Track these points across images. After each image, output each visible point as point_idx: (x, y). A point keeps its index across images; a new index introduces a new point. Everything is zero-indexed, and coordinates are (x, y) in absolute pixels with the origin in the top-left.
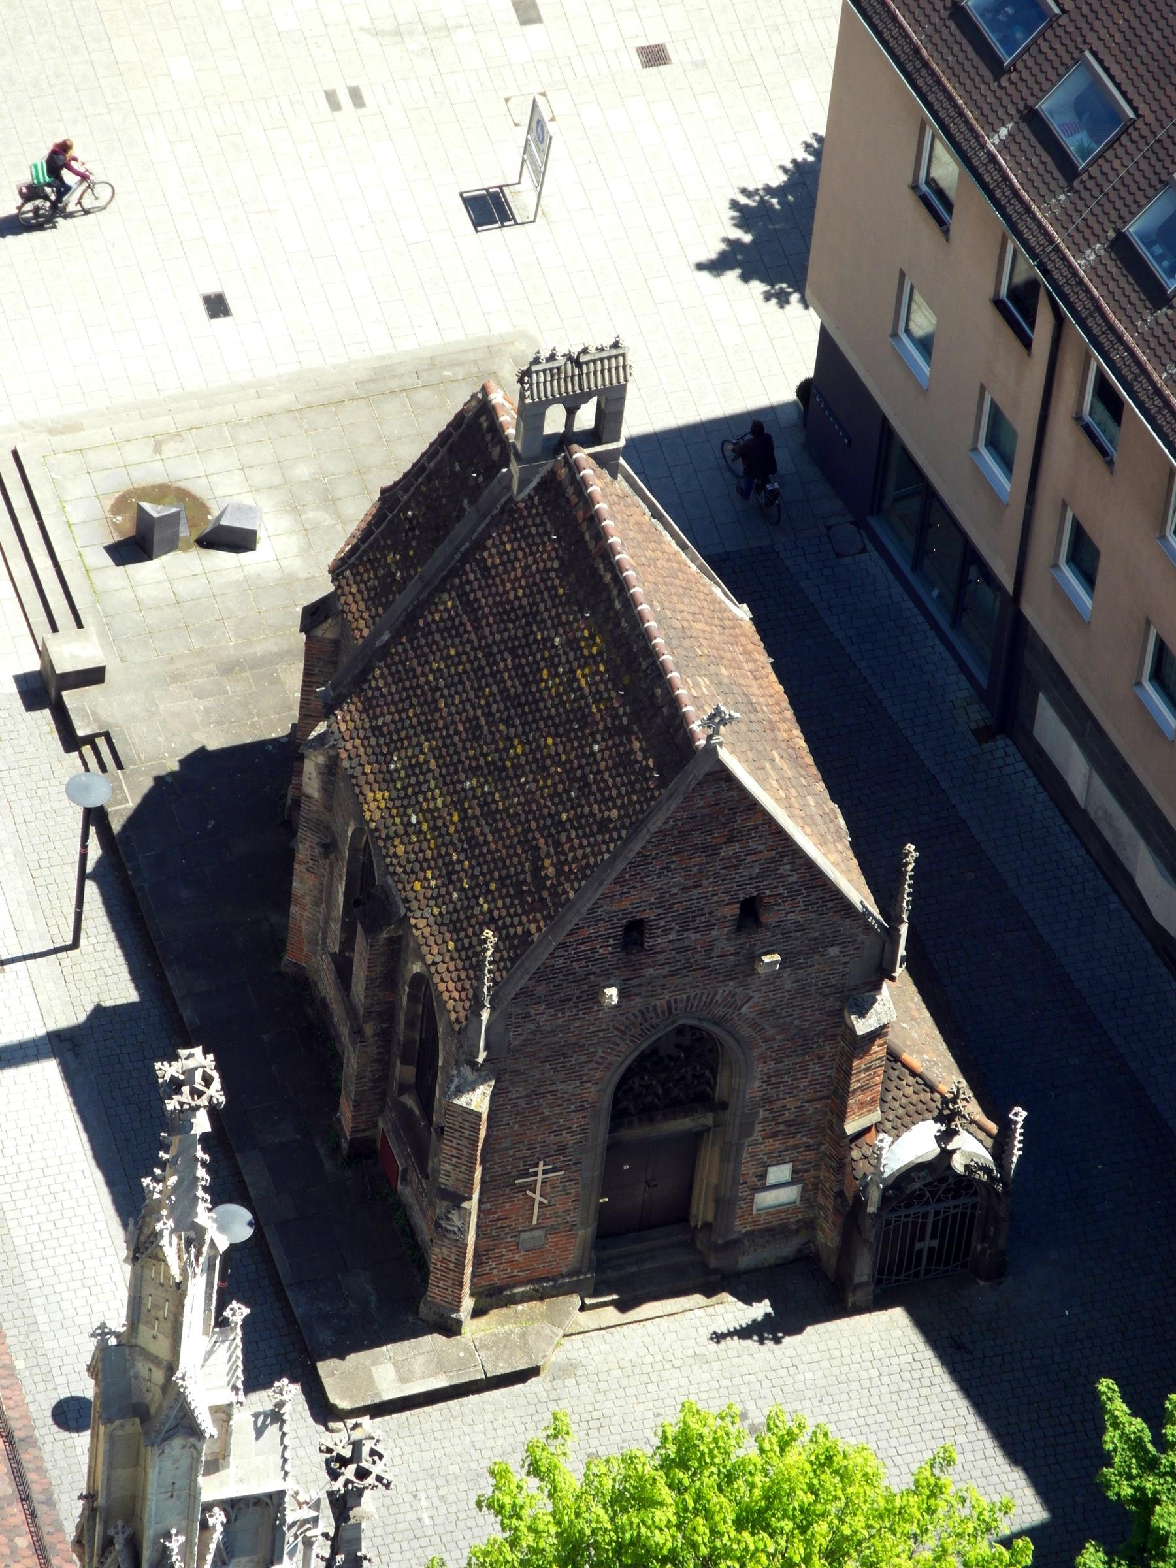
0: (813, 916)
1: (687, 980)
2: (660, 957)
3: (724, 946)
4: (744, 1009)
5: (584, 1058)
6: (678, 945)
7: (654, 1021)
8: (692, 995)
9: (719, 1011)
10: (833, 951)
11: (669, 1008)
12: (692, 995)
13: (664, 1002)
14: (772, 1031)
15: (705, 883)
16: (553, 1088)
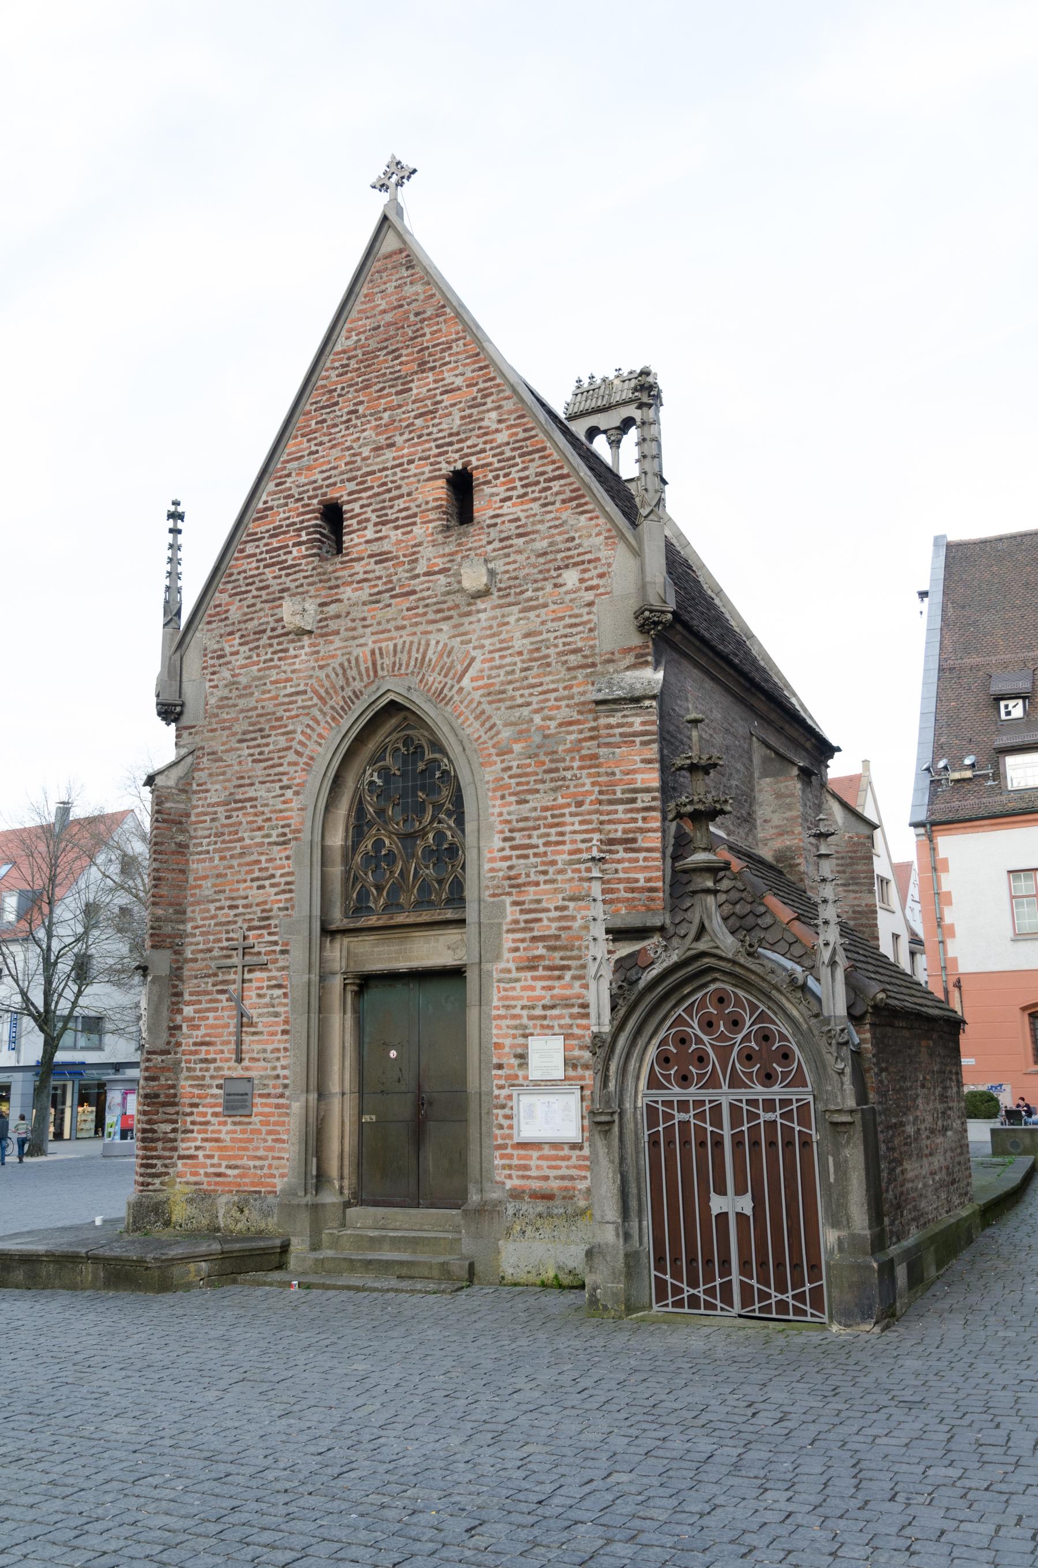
0: (535, 506)
1: (390, 613)
2: (358, 567)
3: (430, 556)
4: (466, 682)
5: (282, 741)
6: (375, 548)
7: (357, 685)
8: (400, 642)
9: (435, 679)
10: (571, 577)
11: (374, 664)
12: (400, 642)
13: (367, 650)
14: (506, 734)
15: (399, 440)
16: (251, 794)
